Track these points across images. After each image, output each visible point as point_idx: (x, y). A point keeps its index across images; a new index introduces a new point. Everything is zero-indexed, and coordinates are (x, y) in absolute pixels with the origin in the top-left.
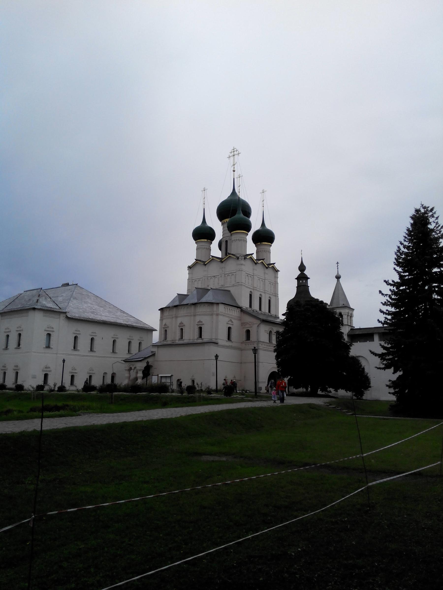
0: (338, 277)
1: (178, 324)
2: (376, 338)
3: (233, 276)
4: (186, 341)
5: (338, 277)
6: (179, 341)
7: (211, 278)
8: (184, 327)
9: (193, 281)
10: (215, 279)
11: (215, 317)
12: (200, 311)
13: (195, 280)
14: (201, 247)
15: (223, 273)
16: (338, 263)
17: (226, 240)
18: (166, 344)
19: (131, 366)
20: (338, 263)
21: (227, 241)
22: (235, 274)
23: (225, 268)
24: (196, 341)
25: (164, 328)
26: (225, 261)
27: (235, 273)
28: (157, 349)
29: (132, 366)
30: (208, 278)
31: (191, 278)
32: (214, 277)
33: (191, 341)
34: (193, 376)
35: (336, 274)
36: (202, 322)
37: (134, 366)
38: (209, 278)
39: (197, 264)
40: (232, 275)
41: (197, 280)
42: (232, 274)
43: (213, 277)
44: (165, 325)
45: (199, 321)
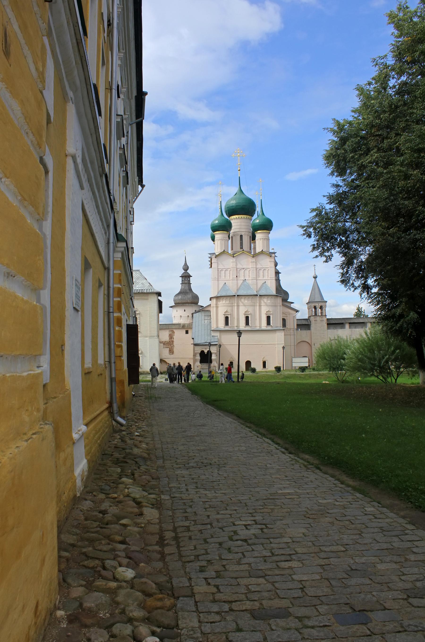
0: (315, 277)
5: (315, 277)
6: (245, 327)
11: (279, 307)
16: (315, 266)
19: (204, 350)
20: (315, 266)
21: (241, 236)
22: (267, 269)
25: (224, 315)
32: (243, 269)
34: (264, 358)
35: (313, 274)
36: (270, 312)
44: (226, 312)
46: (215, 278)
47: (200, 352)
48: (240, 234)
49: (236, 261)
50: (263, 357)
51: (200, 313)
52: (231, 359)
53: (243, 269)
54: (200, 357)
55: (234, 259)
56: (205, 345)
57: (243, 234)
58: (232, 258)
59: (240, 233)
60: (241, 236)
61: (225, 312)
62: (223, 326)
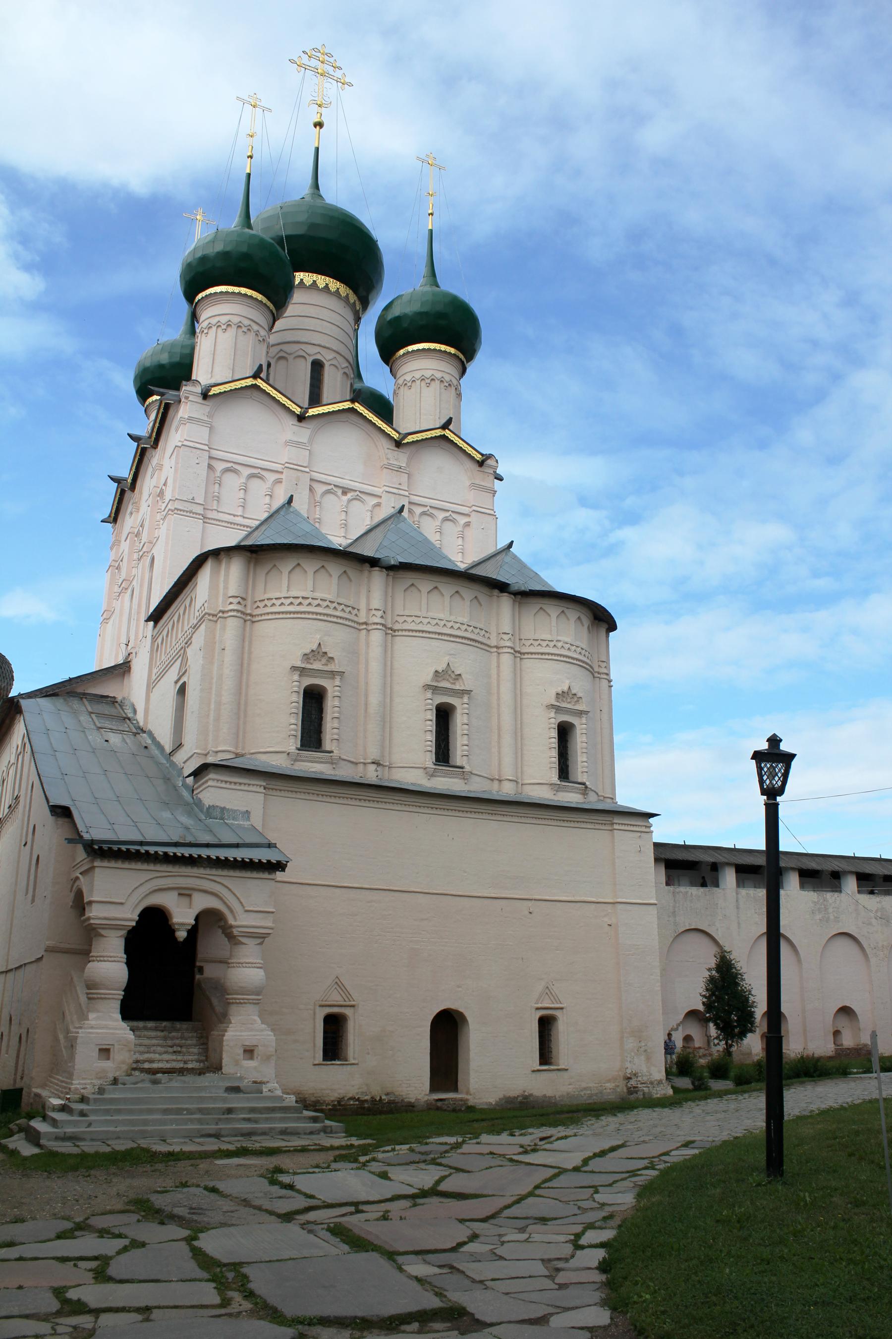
1: (427, 677)
2: (729, 877)
3: (448, 524)
4: (476, 787)
7: (328, 492)
8: (466, 700)
9: (220, 466)
10: (349, 501)
12: (559, 638)
13: (229, 465)
14: (256, 327)
15: (406, 493)
17: (319, 357)
18: (322, 773)
19: (169, 901)
21: (317, 367)
22: (462, 520)
23: (409, 476)
24: (543, 794)
25: (302, 671)
26: (413, 448)
27: (466, 519)
28: (261, 797)
29: (174, 894)
30: (316, 486)
31: (206, 448)
32: (345, 491)
33: (507, 791)
37: (202, 902)
38: (320, 489)
39: (249, 392)
40: (446, 519)
41: (246, 472)
42: (447, 514)
43: (339, 492)
44: (318, 653)
45: (566, 689)
46: (192, 501)
47: (130, 915)
48: (314, 353)
49: (311, 440)
50: (540, 987)
51: (59, 702)
52: (336, 997)
53: (344, 493)
54: (128, 963)
55: (303, 433)
56: (191, 861)
57: (326, 357)
58: (290, 423)
59: (318, 349)
60: (317, 367)
61: (306, 657)
62: (292, 745)
